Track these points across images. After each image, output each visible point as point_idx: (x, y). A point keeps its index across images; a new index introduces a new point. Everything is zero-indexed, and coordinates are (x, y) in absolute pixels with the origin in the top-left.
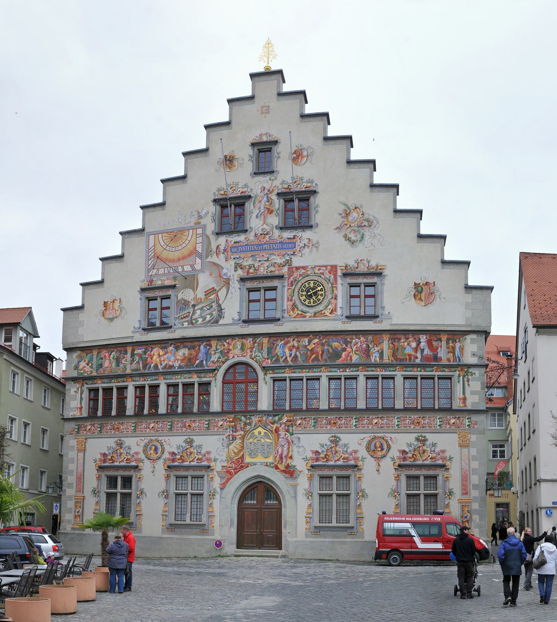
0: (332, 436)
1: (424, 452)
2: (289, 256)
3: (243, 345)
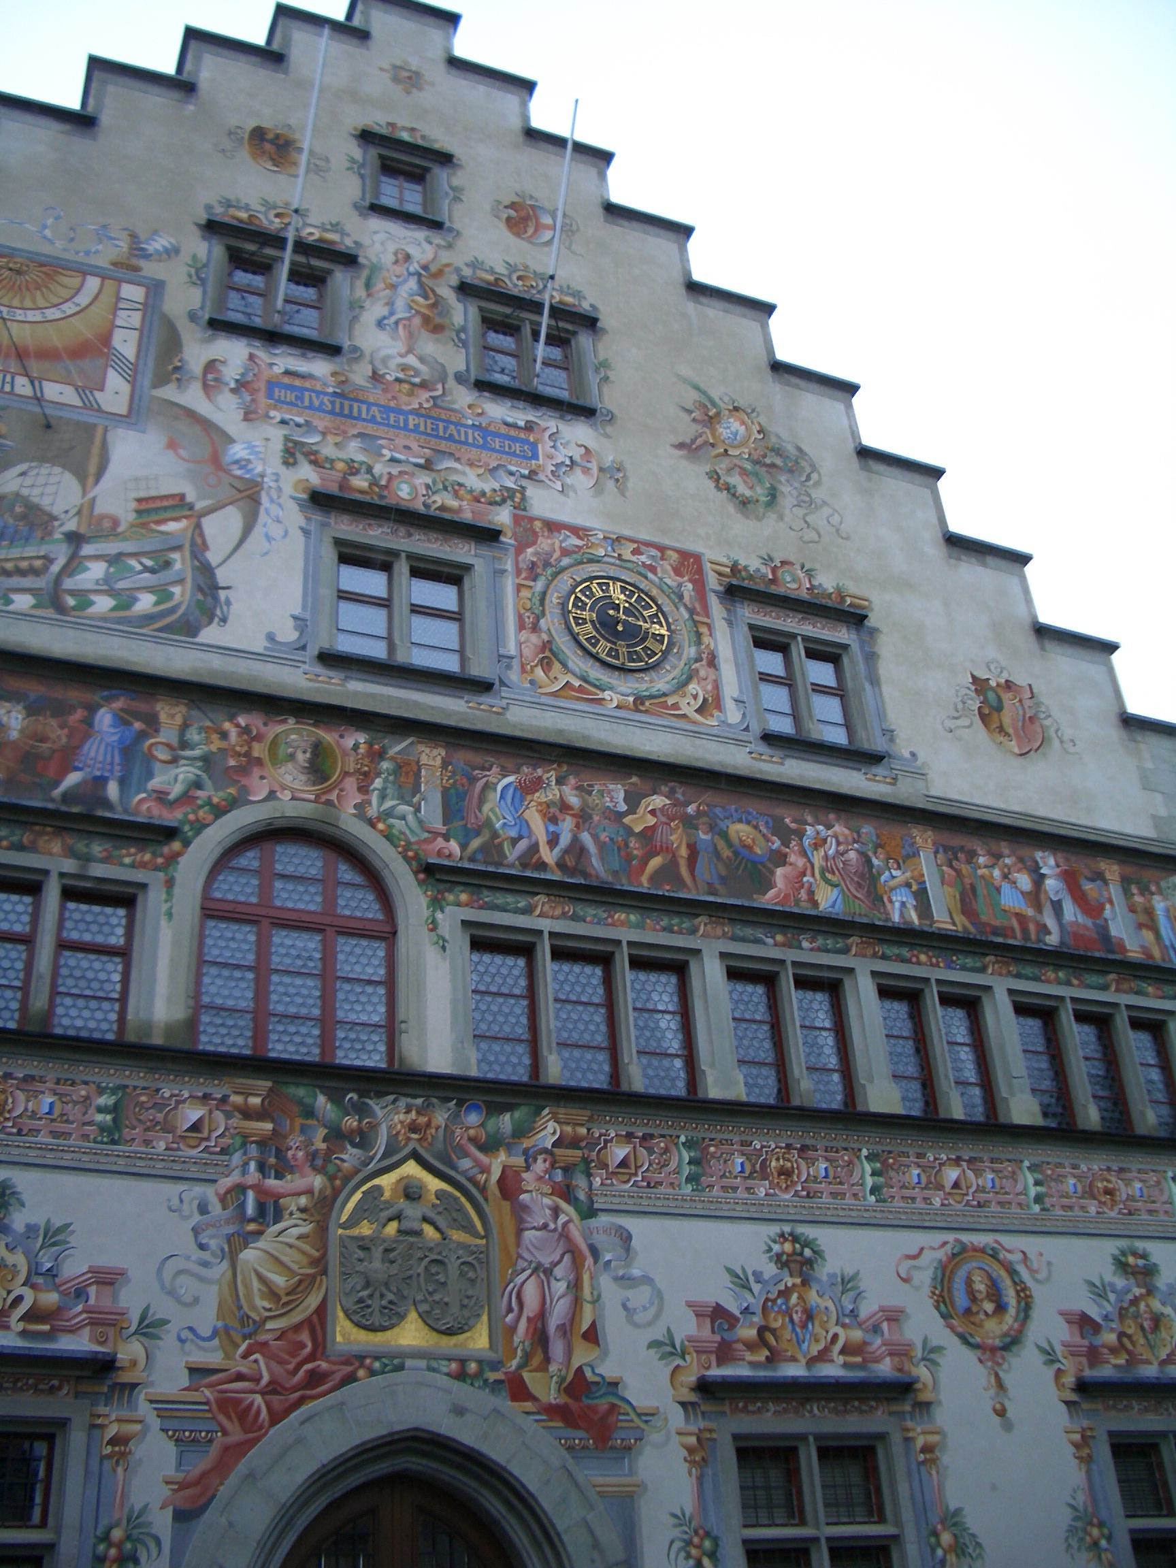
0: (782, 1235)
2: (513, 478)
3: (319, 752)
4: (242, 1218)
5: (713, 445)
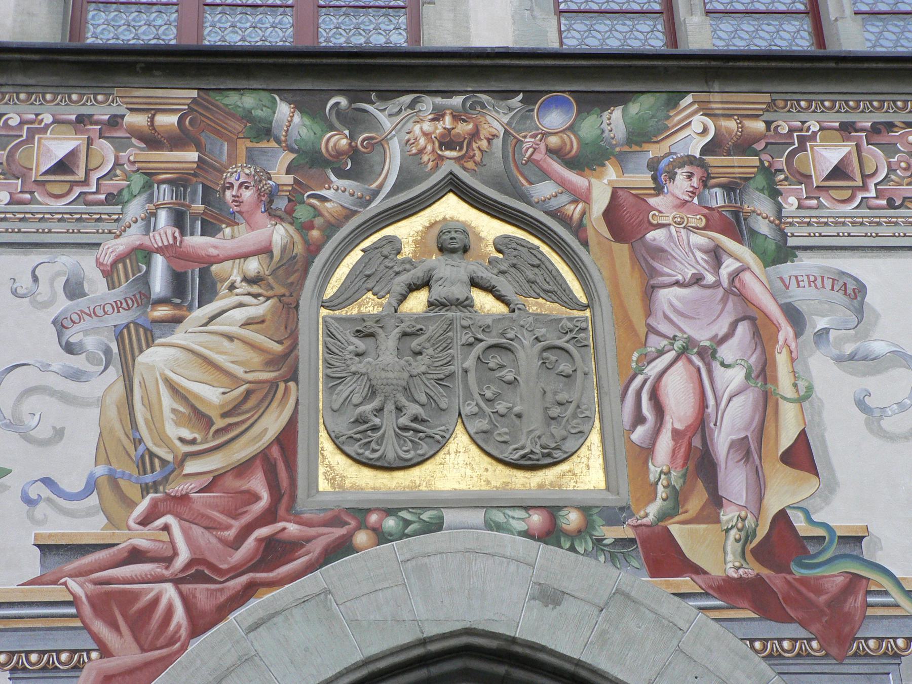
4: (144, 297)
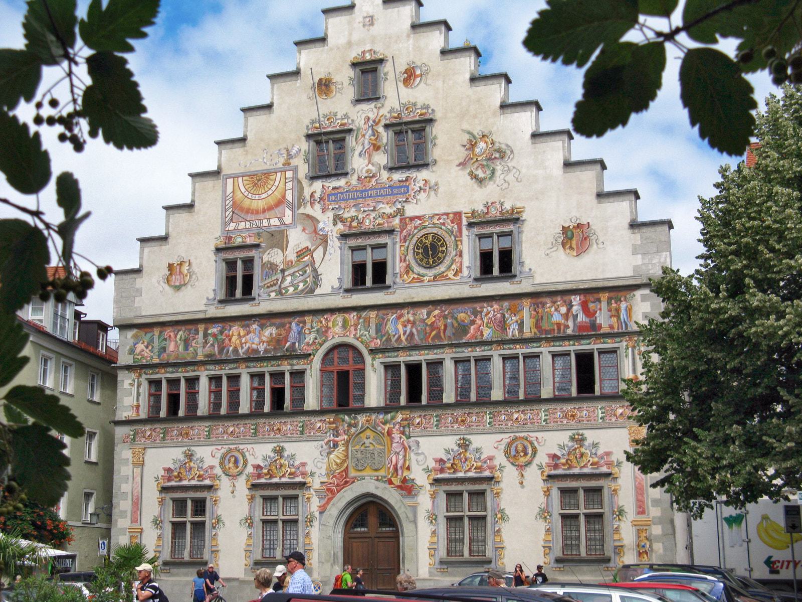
1: (582, 455)
3: (345, 322)
5: (472, 159)
